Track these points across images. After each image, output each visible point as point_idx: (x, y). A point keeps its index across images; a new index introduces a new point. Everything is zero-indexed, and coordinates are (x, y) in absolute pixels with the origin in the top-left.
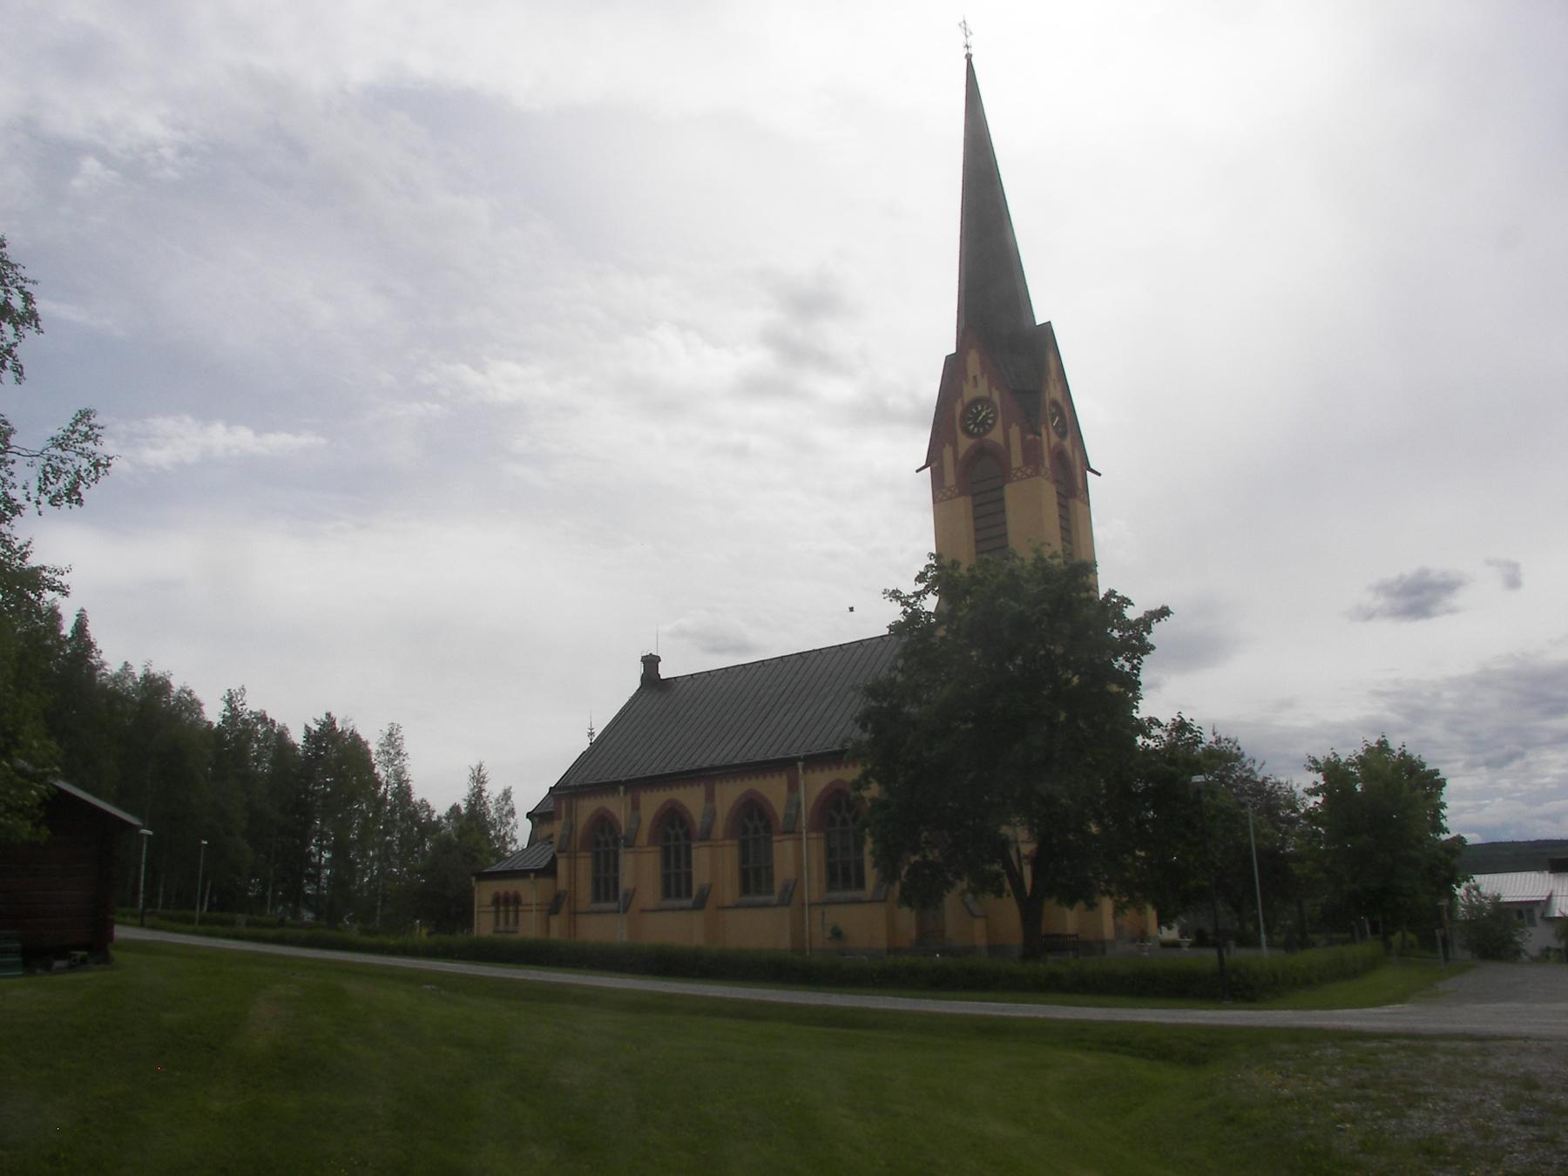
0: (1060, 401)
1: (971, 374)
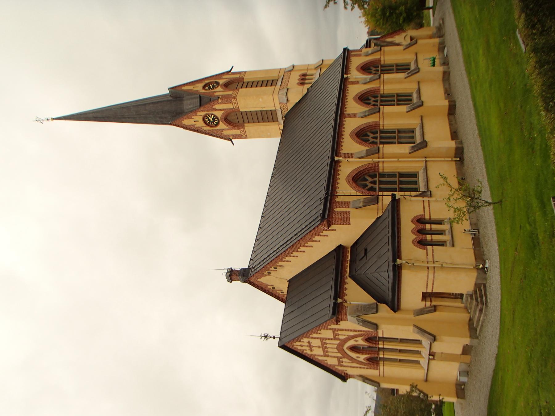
0: (203, 84)
1: (194, 123)
